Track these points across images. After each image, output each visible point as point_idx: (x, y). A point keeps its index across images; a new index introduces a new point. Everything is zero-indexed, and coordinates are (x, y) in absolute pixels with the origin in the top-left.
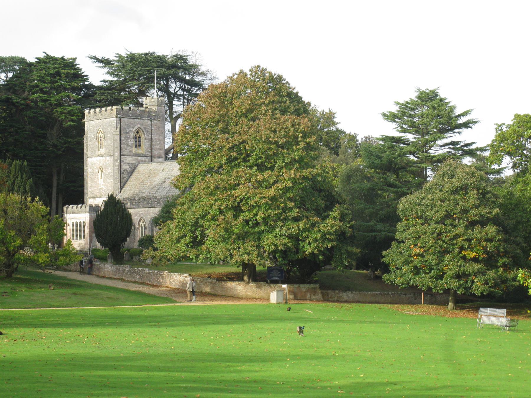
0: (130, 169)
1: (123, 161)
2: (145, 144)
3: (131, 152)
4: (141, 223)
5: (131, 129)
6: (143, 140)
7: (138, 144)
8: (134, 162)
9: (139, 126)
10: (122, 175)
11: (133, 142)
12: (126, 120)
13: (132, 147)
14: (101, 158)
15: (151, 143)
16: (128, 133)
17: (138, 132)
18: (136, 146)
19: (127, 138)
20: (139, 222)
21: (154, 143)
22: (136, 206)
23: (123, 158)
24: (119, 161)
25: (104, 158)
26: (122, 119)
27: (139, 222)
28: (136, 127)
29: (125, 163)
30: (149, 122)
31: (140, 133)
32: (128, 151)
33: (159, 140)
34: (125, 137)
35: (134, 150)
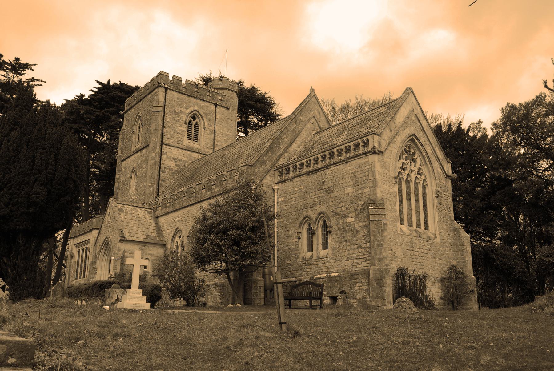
0: (176, 168)
1: (166, 153)
2: (204, 136)
3: (179, 142)
4: (177, 239)
5: (183, 110)
6: (201, 130)
7: (193, 134)
8: (185, 159)
9: (196, 108)
10: (162, 174)
11: (185, 128)
12: (176, 95)
13: (183, 136)
14: (136, 155)
15: (214, 137)
16: (177, 114)
17: (194, 118)
18: (189, 138)
19: (175, 121)
20: (174, 237)
21: (218, 138)
22: (171, 209)
23: (166, 149)
24: (158, 150)
25: (139, 153)
26: (169, 91)
27: (174, 237)
28: (192, 109)
29: (168, 157)
30: (213, 107)
31: (197, 120)
32: (175, 139)
33: (226, 135)
34: (173, 119)
35: (186, 142)
